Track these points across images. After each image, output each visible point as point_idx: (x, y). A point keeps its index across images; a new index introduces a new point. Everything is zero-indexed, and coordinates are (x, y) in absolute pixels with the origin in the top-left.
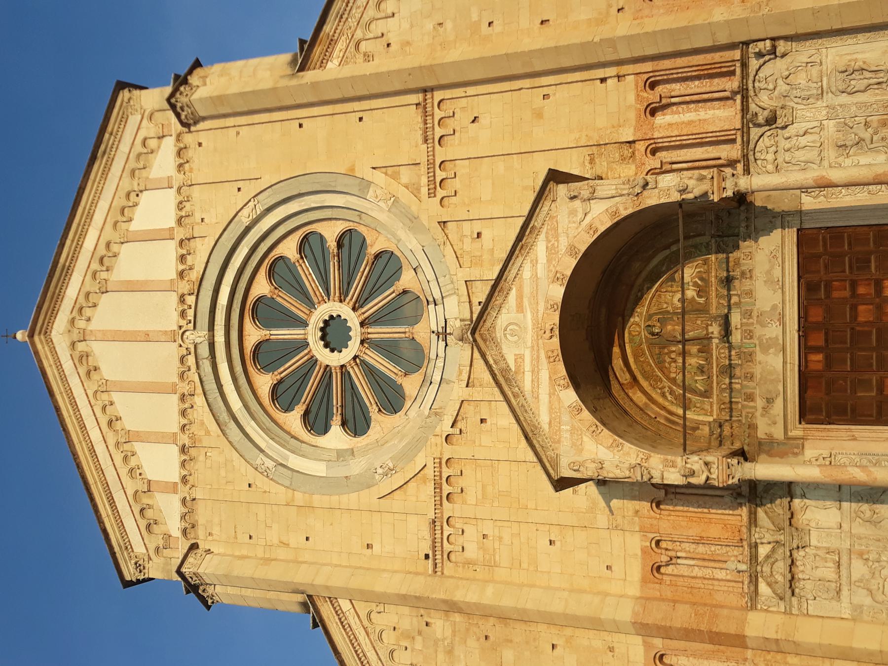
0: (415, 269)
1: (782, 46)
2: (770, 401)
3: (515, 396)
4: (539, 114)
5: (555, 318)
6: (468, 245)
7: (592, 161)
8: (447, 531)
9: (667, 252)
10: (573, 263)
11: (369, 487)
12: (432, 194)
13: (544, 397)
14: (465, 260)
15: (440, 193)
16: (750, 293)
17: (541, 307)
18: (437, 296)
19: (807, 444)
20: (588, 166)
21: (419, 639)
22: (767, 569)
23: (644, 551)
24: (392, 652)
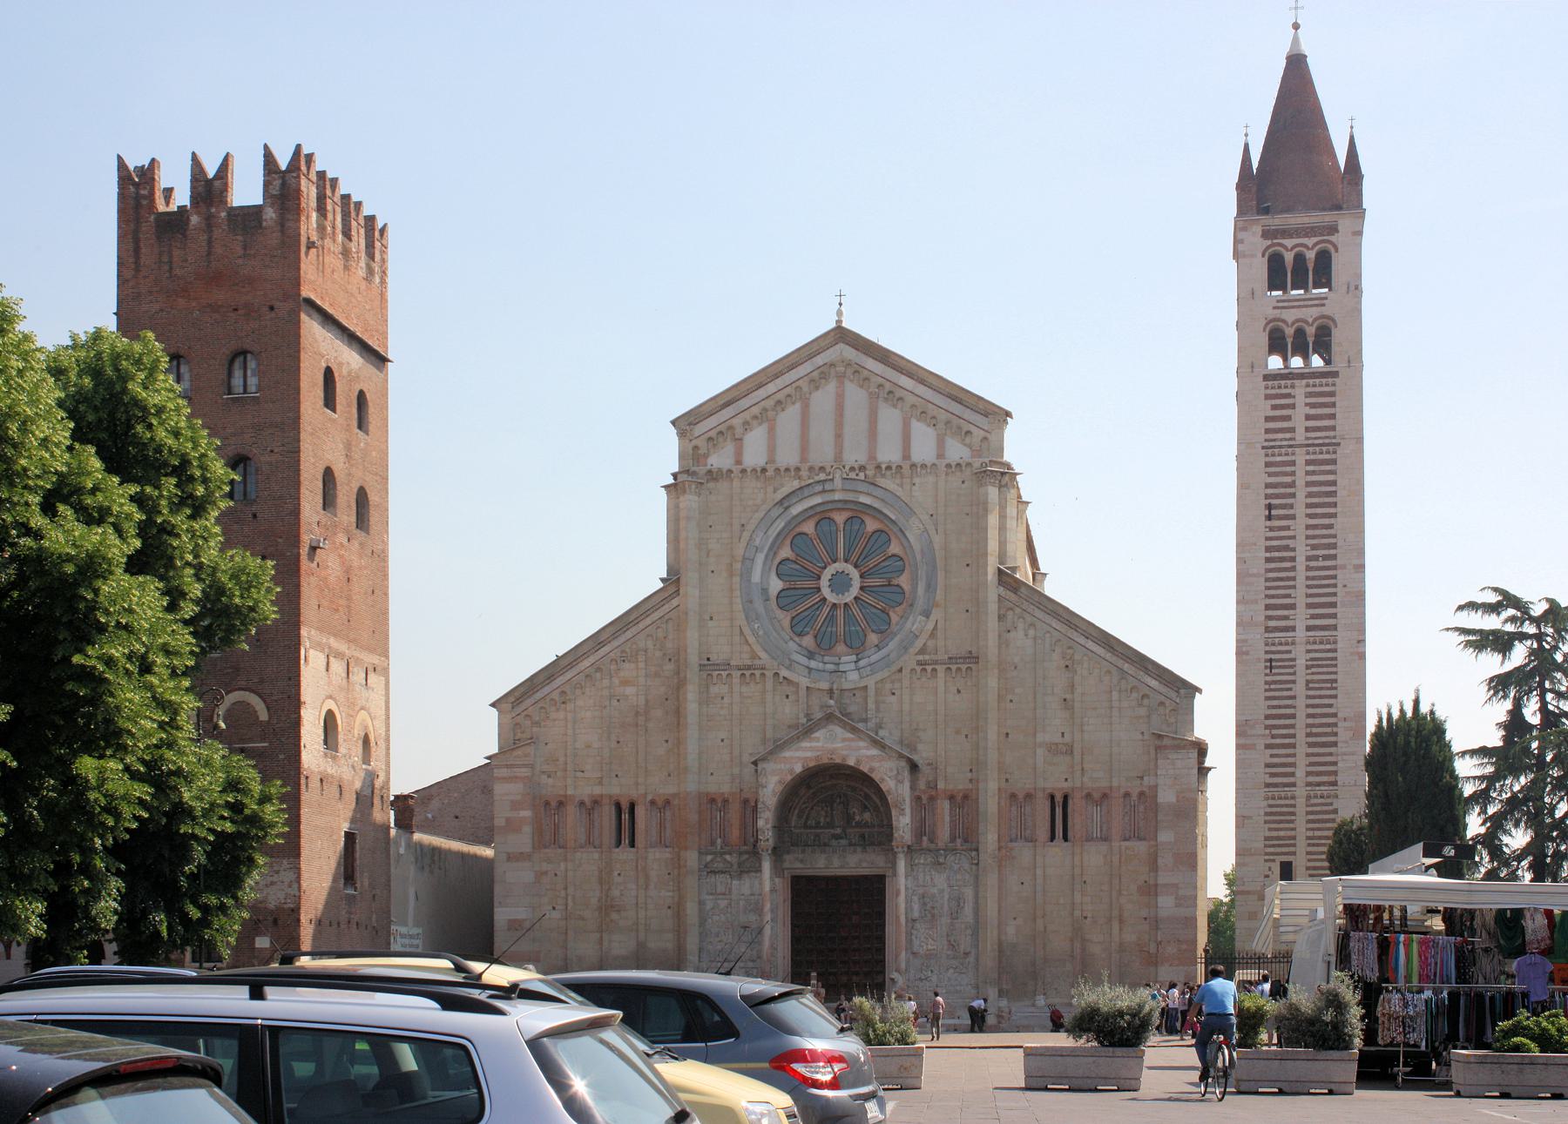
0: (877, 646)
1: (974, 867)
2: (802, 861)
3: (798, 738)
4: (958, 732)
5: (838, 761)
6: (888, 686)
7: (929, 764)
8: (724, 674)
9: (879, 804)
10: (866, 770)
11: (747, 618)
12: (919, 663)
13: (798, 754)
14: (879, 685)
15: (919, 668)
16: (855, 851)
17: (845, 752)
18: (862, 663)
19: (781, 880)
20: (927, 762)
21: (658, 654)
22: (719, 859)
23: (723, 794)
24: (652, 636)
